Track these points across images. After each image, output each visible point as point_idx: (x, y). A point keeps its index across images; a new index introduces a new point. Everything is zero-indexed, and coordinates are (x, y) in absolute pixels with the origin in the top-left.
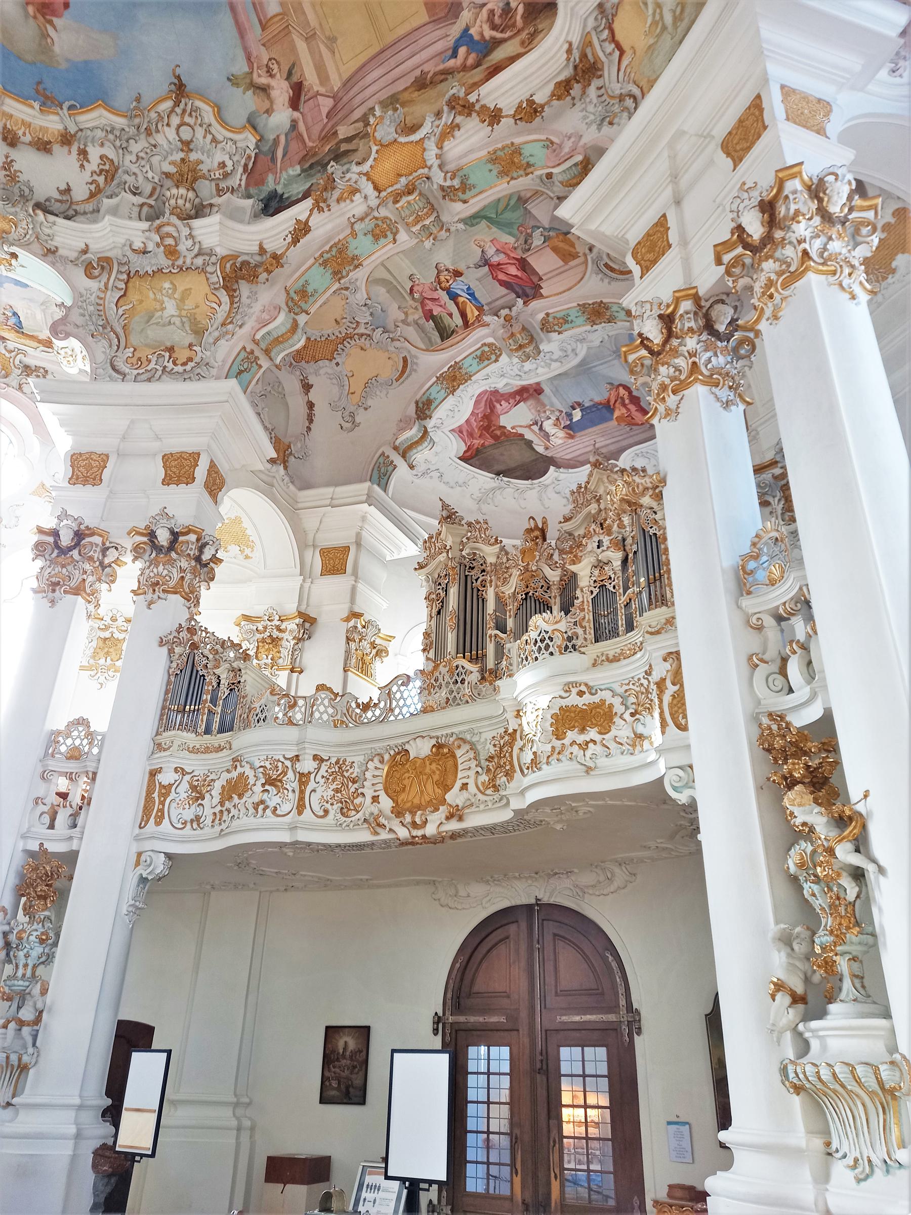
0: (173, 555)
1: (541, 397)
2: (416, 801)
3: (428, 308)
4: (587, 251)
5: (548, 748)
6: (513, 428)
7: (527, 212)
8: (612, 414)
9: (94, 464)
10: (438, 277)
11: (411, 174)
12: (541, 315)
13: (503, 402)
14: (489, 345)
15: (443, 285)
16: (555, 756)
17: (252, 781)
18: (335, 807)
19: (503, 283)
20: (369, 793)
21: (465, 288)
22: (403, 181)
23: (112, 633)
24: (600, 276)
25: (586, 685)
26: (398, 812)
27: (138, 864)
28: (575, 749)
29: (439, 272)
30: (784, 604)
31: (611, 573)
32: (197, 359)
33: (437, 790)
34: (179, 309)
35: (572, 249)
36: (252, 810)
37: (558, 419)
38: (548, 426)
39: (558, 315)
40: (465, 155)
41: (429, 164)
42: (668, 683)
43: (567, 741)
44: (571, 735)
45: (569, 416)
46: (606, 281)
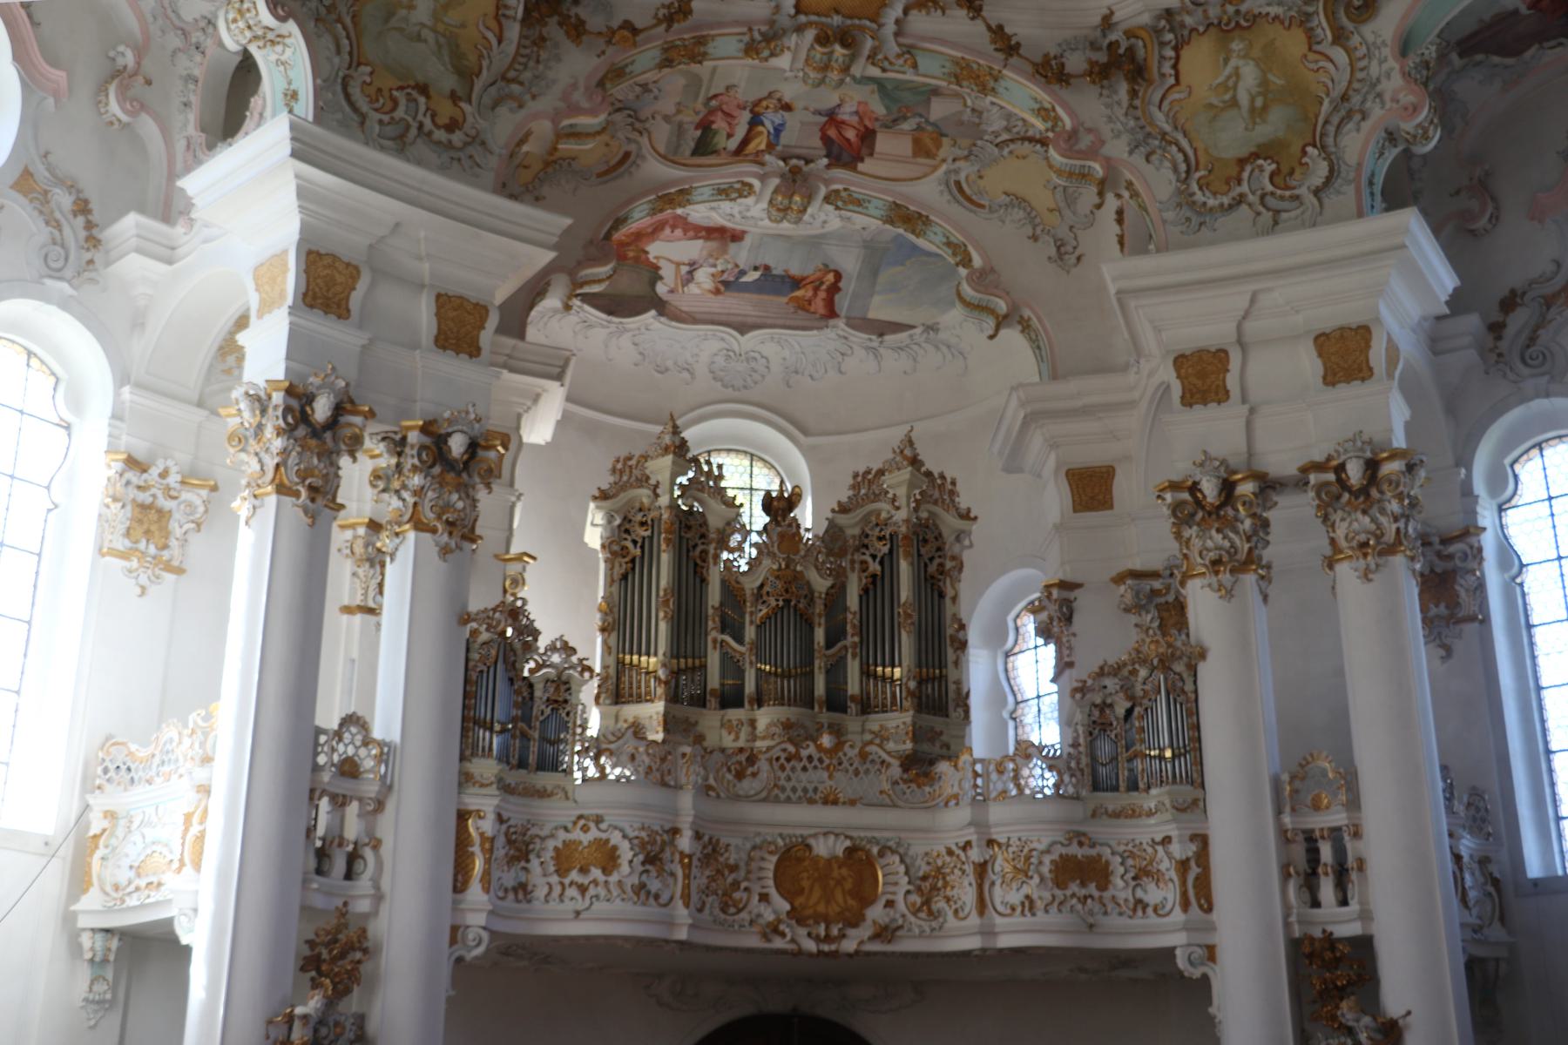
0: (464, 475)
1: (733, 247)
2: (821, 908)
3: (712, 118)
4: (950, 160)
5: (1047, 895)
6: (656, 258)
7: (928, 101)
8: (793, 291)
9: (339, 279)
10: (760, 101)
11: (851, 17)
12: (839, 187)
13: (679, 232)
14: (744, 184)
15: (757, 109)
16: (1056, 904)
17: (626, 852)
18: (710, 899)
19: (826, 140)
20: (756, 889)
21: (778, 121)
22: (837, 20)
23: (154, 496)
24: (942, 188)
25: (1084, 834)
26: (796, 915)
27: (453, 941)
28: (1074, 901)
29: (770, 95)
30: (1322, 830)
31: (1113, 719)
32: (467, 126)
33: (851, 902)
34: (436, 16)
35: (934, 150)
36: (631, 894)
37: (723, 272)
38: (703, 276)
39: (855, 195)
40: (933, 40)
41: (882, 20)
42: (1193, 864)
43: (1069, 892)
44: (1074, 887)
45: (743, 273)
46: (947, 197)
